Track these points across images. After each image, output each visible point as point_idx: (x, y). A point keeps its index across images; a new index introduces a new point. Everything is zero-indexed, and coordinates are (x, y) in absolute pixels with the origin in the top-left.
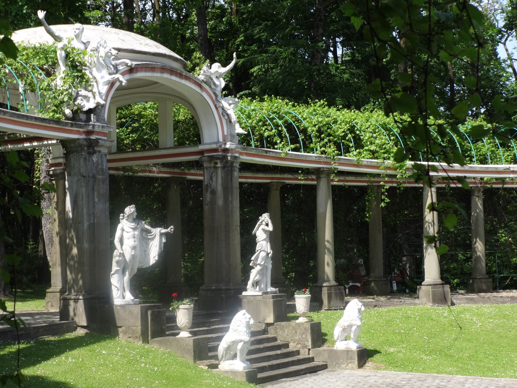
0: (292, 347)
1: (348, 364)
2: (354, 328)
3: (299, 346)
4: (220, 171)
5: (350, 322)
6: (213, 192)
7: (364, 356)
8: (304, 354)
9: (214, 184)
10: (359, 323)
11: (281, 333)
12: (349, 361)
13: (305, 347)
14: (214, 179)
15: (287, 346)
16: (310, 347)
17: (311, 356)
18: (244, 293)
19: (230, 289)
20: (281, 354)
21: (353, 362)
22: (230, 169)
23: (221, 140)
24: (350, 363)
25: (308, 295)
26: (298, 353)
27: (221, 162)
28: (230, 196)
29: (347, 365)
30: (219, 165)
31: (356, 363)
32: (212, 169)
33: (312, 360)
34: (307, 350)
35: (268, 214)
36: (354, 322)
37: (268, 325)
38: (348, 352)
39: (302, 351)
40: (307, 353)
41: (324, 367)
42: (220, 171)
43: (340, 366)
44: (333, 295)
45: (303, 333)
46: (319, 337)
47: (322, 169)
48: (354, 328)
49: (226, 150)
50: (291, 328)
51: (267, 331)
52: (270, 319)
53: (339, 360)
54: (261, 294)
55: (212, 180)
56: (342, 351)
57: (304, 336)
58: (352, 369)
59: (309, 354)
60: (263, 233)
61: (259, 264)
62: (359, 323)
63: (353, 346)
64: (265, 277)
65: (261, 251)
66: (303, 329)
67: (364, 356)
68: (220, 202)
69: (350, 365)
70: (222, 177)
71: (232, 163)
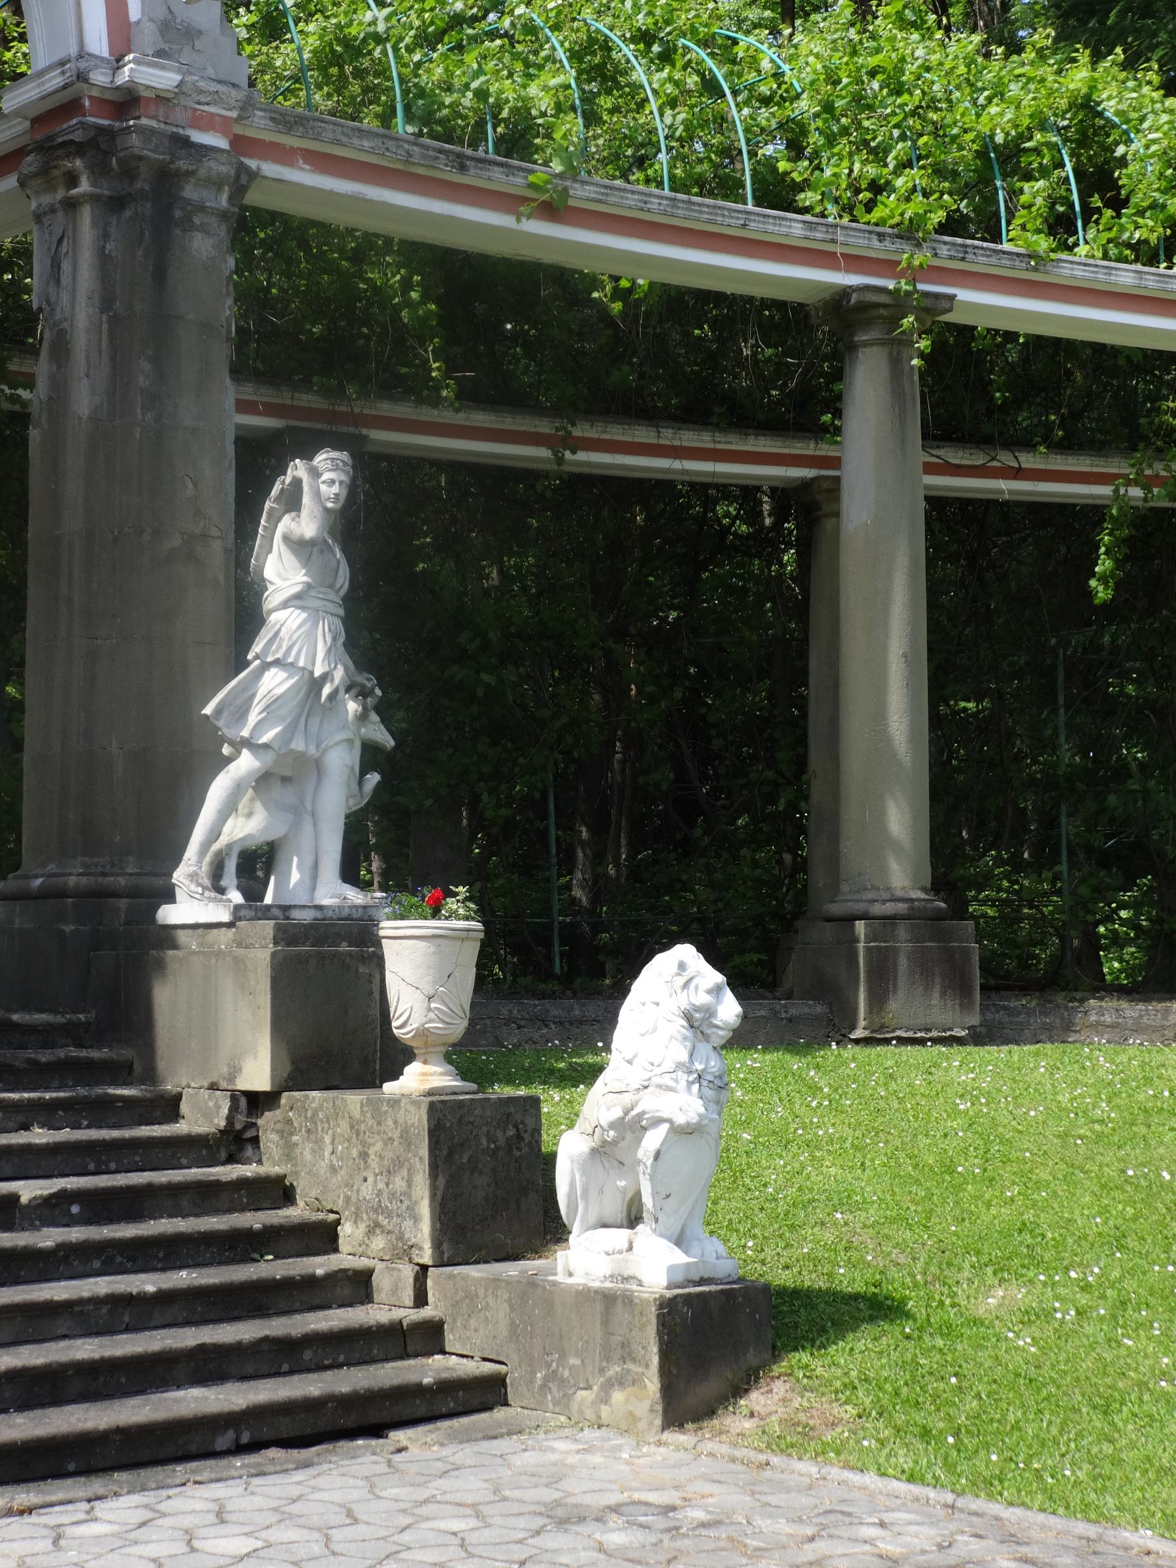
0: (355, 1246)
1: (608, 1386)
2: (653, 1140)
3: (379, 1243)
4: (86, 214)
5: (627, 1099)
6: (61, 350)
7: (718, 1344)
8: (392, 1304)
9: (65, 298)
10: (687, 1106)
11: (308, 1156)
12: (615, 1369)
13: (405, 1251)
14: (66, 266)
15: (323, 1236)
16: (426, 1257)
17: (427, 1312)
18: (170, 914)
19: (115, 894)
20: (165, 1298)
21: (637, 1381)
22: (147, 208)
23: (98, 41)
24: (621, 1382)
25: (460, 920)
26: (359, 1285)
27: (99, 170)
28: (145, 365)
29: (605, 1399)
30: (84, 186)
31: (653, 1385)
32: (60, 215)
33: (429, 1337)
34: (408, 1273)
35: (344, 456)
36: (650, 1104)
37: (257, 1102)
38: (610, 1302)
39: (382, 1282)
40: (408, 1296)
41: (482, 1394)
42: (86, 214)
43: (568, 1397)
44: (903, 963)
45: (398, 1163)
46: (497, 1194)
47: (854, 298)
48: (653, 1140)
49: (127, 101)
50: (343, 1127)
51: (255, 1140)
52: (257, 1075)
53: (563, 1356)
54: (225, 917)
55: (58, 282)
56: (586, 1295)
57: (399, 1183)
58: (628, 1427)
59: (421, 1299)
60: (290, 559)
61: (247, 743)
62: (687, 1106)
63: (655, 1264)
64: (308, 819)
65: (266, 666)
66: (396, 1135)
67: (718, 1344)
68: (84, 400)
69: (618, 1396)
70: (103, 258)
71: (167, 180)
